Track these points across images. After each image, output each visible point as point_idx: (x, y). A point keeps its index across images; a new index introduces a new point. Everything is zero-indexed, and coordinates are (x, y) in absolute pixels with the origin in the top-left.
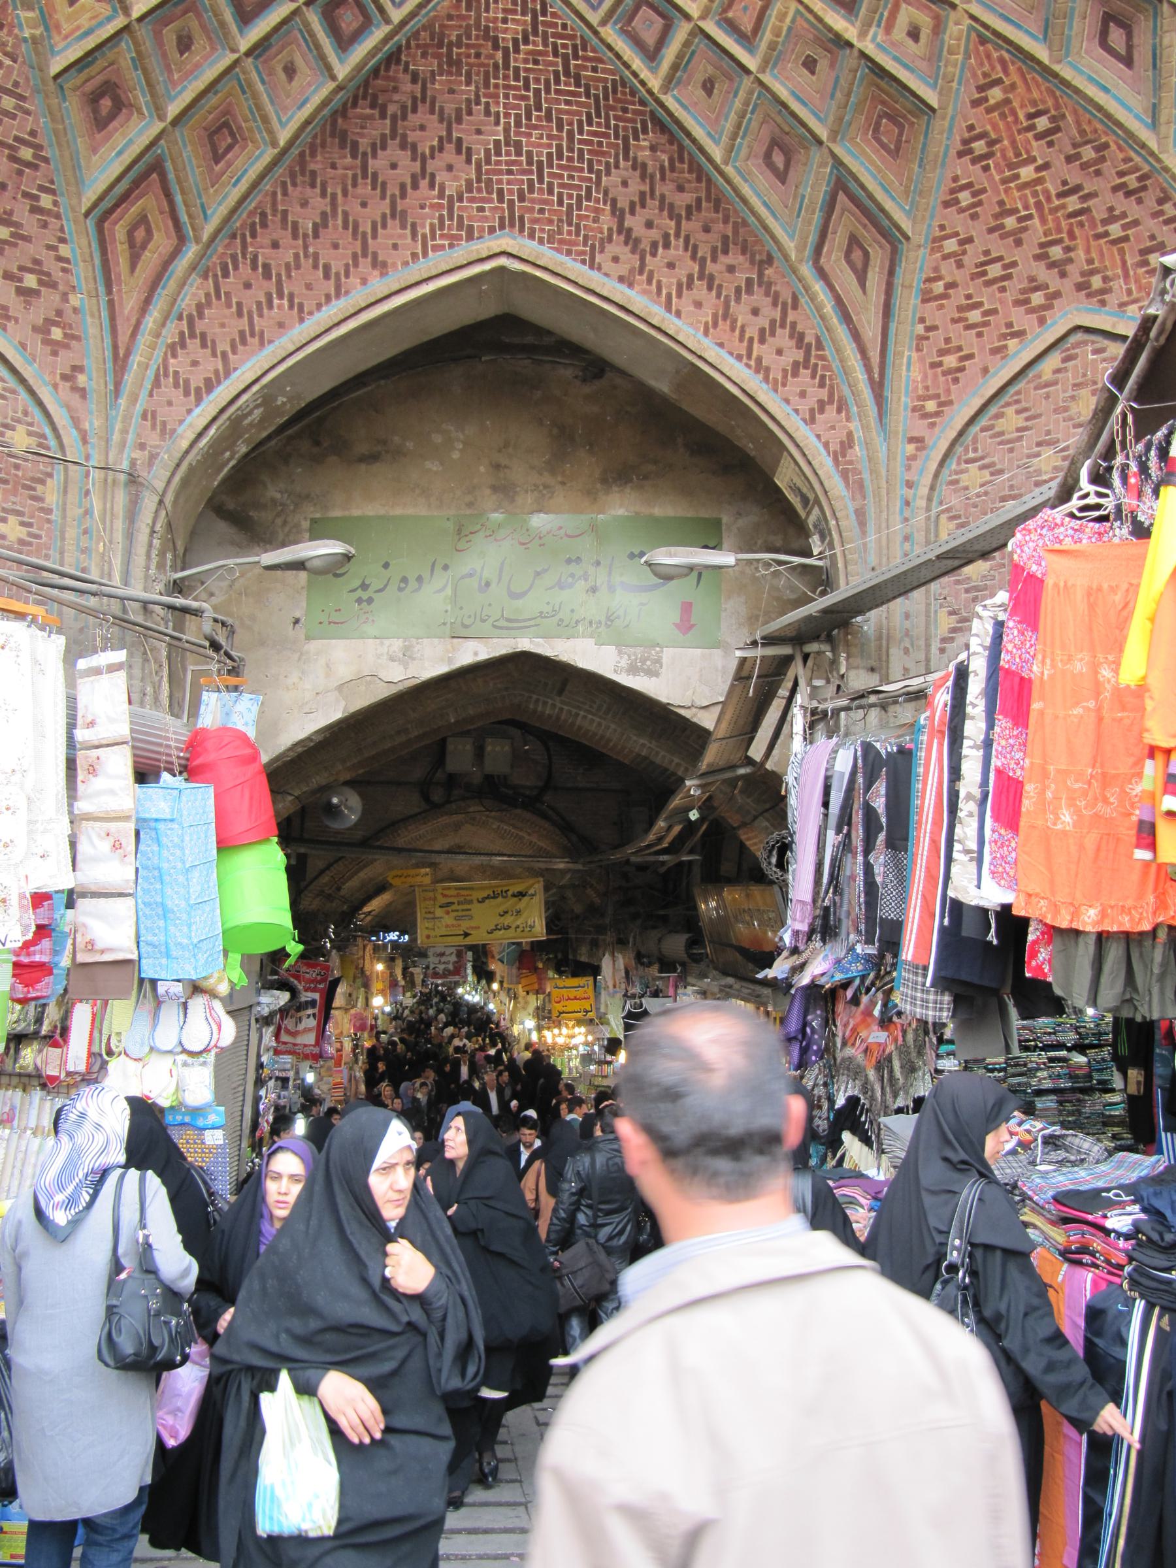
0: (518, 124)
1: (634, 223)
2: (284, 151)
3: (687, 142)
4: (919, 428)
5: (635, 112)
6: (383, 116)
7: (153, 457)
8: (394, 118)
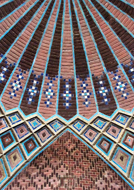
0: (72, 169)
2: (12, 177)
3: (117, 172)
5: (103, 165)
6: (38, 168)
8: (40, 168)
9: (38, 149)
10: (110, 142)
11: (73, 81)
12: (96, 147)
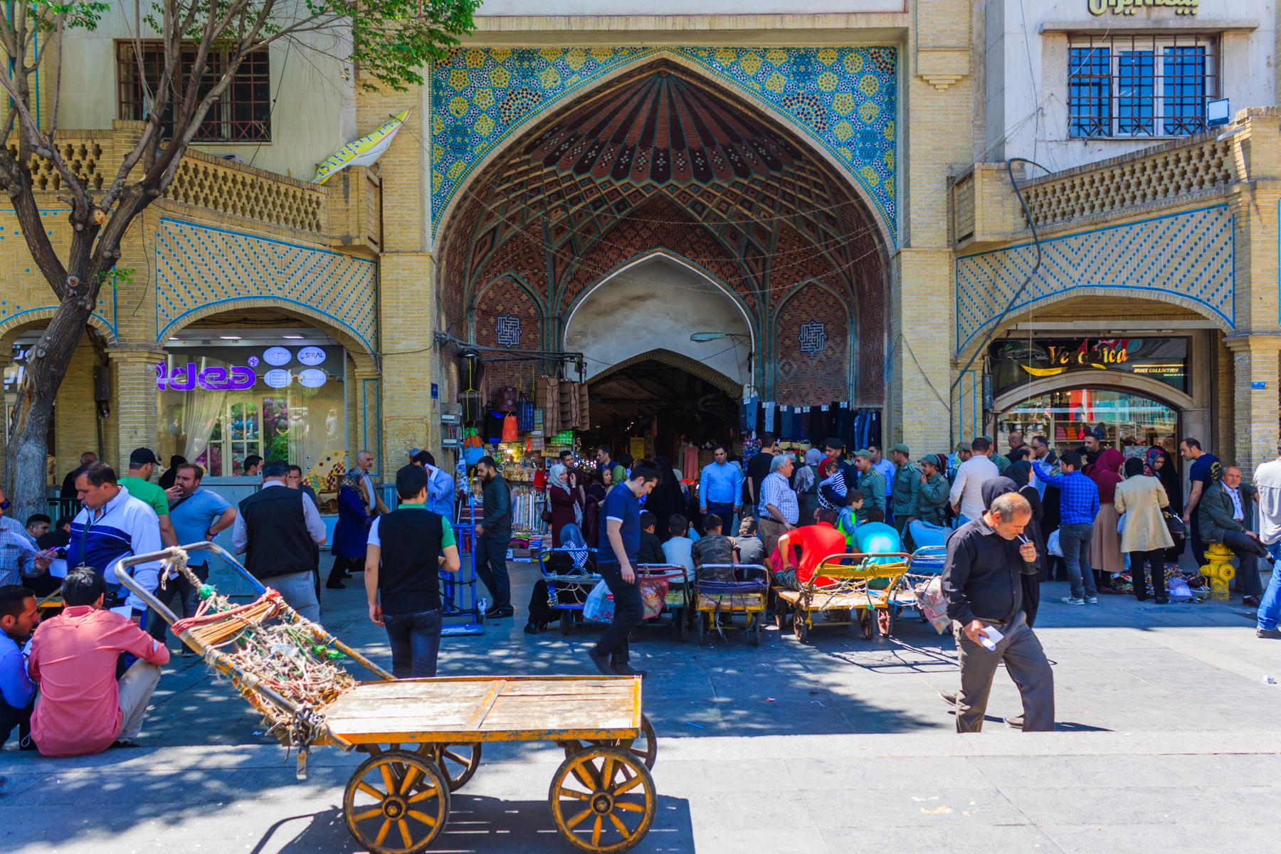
1: (696, 247)
4: (773, 302)
7: (564, 312)
9: (628, 210)
10: (704, 207)
11: (668, 151)
12: (689, 209)
